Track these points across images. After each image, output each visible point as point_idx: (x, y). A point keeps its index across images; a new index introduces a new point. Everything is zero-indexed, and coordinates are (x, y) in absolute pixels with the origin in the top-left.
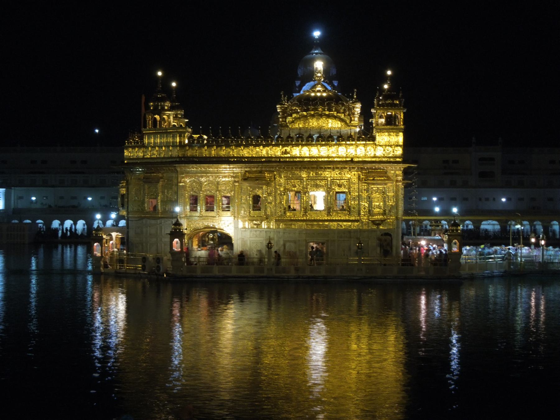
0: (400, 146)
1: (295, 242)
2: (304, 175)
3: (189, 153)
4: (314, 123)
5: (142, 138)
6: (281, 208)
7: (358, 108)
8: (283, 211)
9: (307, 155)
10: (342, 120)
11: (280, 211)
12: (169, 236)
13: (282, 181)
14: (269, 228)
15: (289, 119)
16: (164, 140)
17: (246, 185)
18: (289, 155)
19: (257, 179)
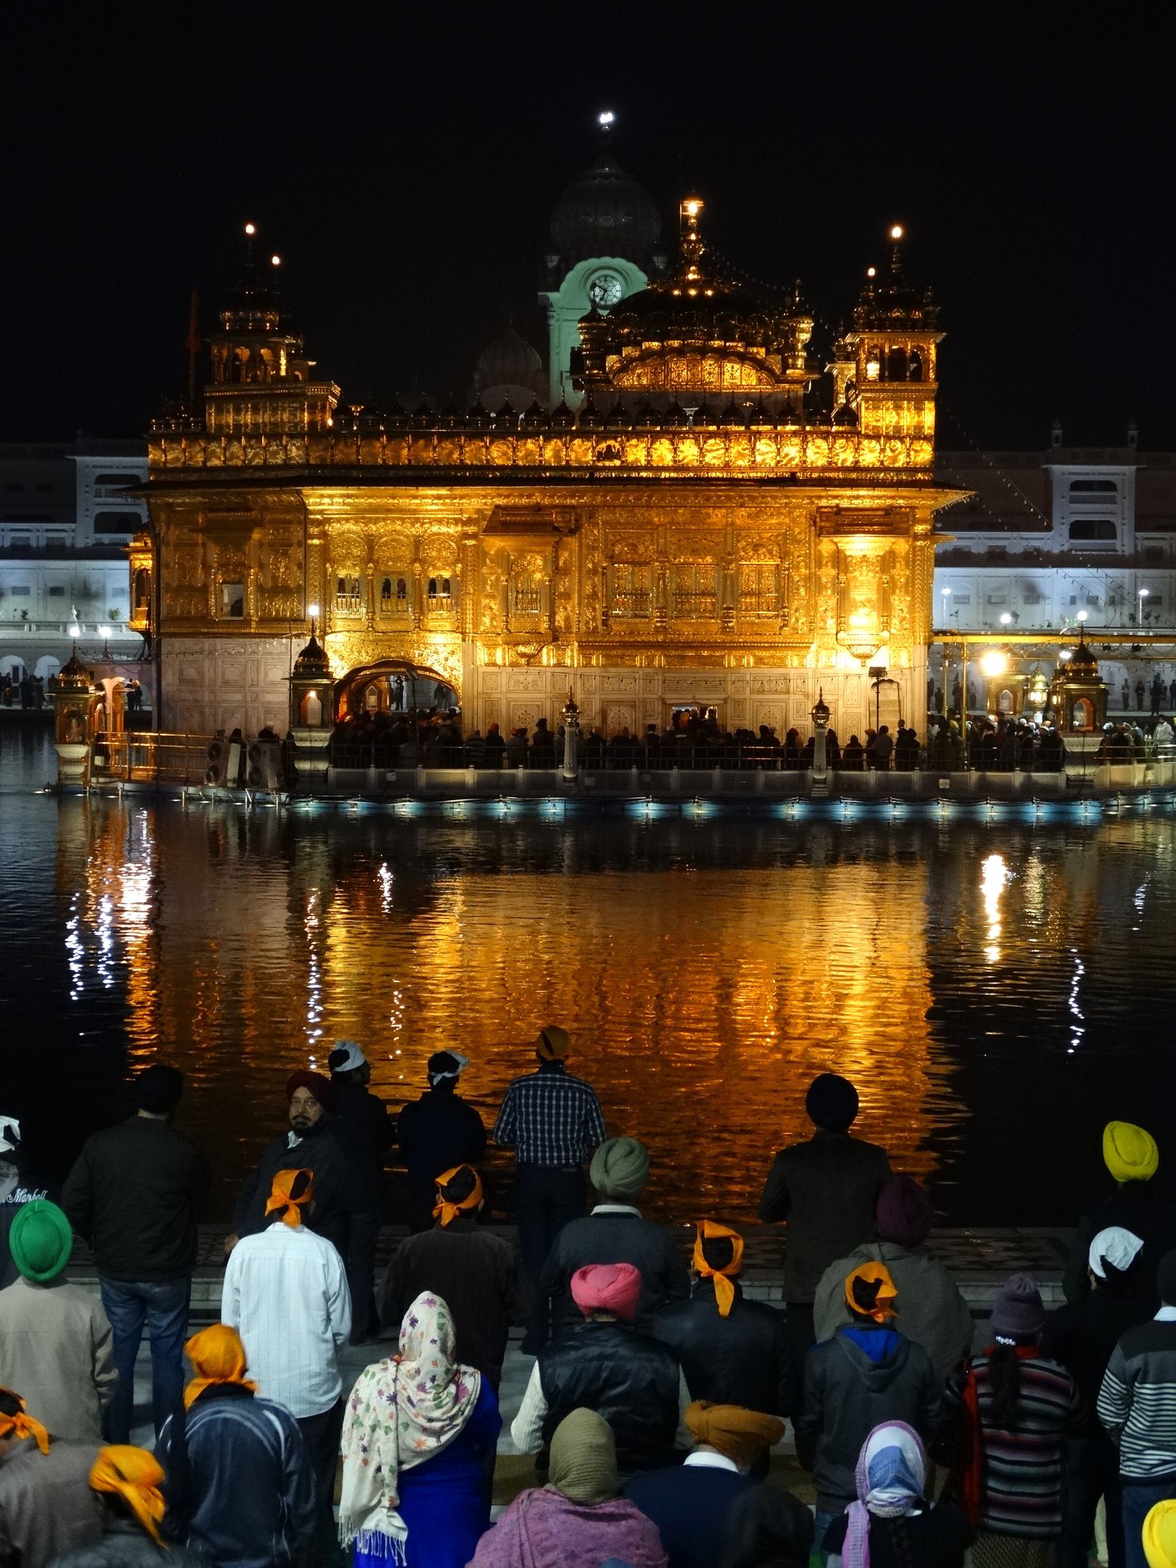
0: (926, 438)
1: (633, 705)
4: (681, 373)
5: (201, 414)
6: (594, 610)
7: (805, 331)
10: (759, 365)
11: (594, 619)
14: (559, 665)
15: (612, 360)
16: (264, 418)
17: (496, 544)
18: (617, 463)
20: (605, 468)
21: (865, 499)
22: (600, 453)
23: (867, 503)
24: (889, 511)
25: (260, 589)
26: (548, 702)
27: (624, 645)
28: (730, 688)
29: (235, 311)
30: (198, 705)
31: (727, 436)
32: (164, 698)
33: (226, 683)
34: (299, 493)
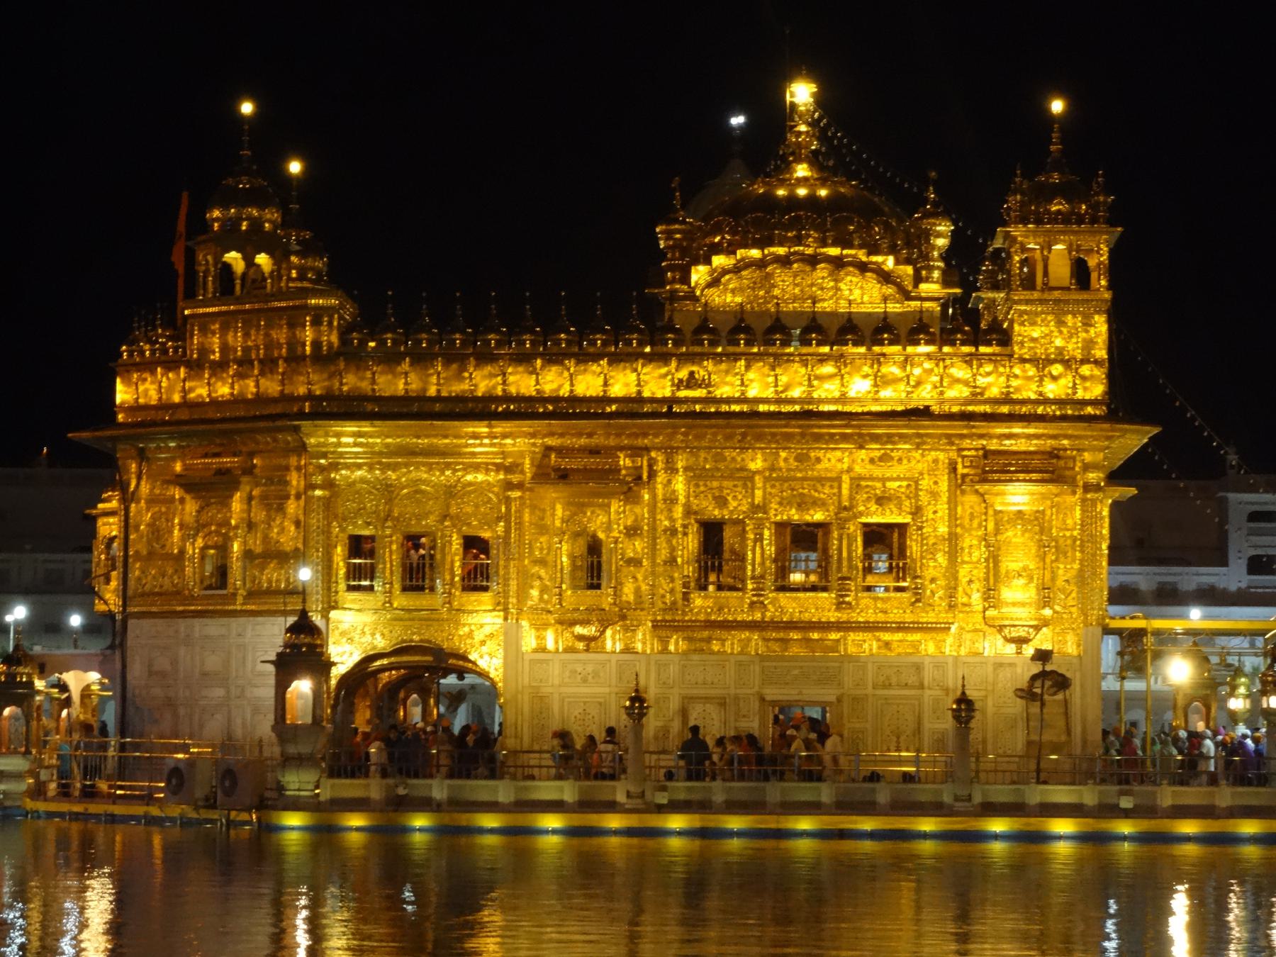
1: (722, 703)
2: (757, 463)
3: (351, 382)
5: (179, 330)
6: (672, 580)
7: (942, 235)
8: (679, 588)
9: (769, 393)
10: (886, 277)
11: (672, 591)
12: (271, 668)
13: (680, 485)
14: (627, 650)
15: (699, 274)
18: (699, 393)
19: (588, 474)
20: (686, 400)
21: (1021, 438)
22: (681, 381)
23: (1021, 445)
24: (1053, 454)
25: (248, 555)
26: (613, 696)
27: (710, 625)
28: (848, 681)
29: (225, 206)
30: (170, 703)
31: (840, 359)
32: (129, 695)
33: (205, 674)
34: (296, 429)
